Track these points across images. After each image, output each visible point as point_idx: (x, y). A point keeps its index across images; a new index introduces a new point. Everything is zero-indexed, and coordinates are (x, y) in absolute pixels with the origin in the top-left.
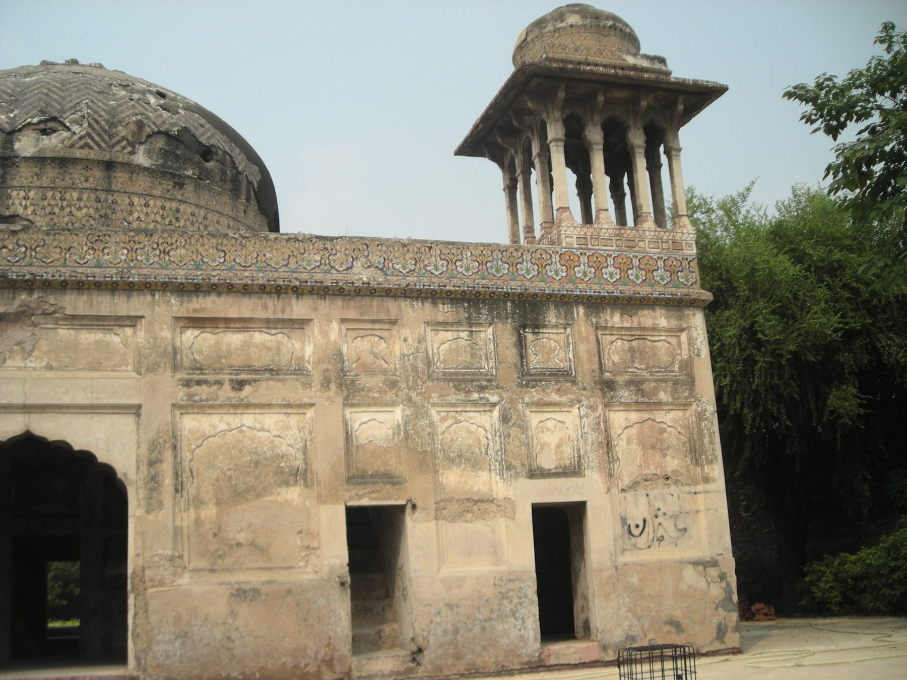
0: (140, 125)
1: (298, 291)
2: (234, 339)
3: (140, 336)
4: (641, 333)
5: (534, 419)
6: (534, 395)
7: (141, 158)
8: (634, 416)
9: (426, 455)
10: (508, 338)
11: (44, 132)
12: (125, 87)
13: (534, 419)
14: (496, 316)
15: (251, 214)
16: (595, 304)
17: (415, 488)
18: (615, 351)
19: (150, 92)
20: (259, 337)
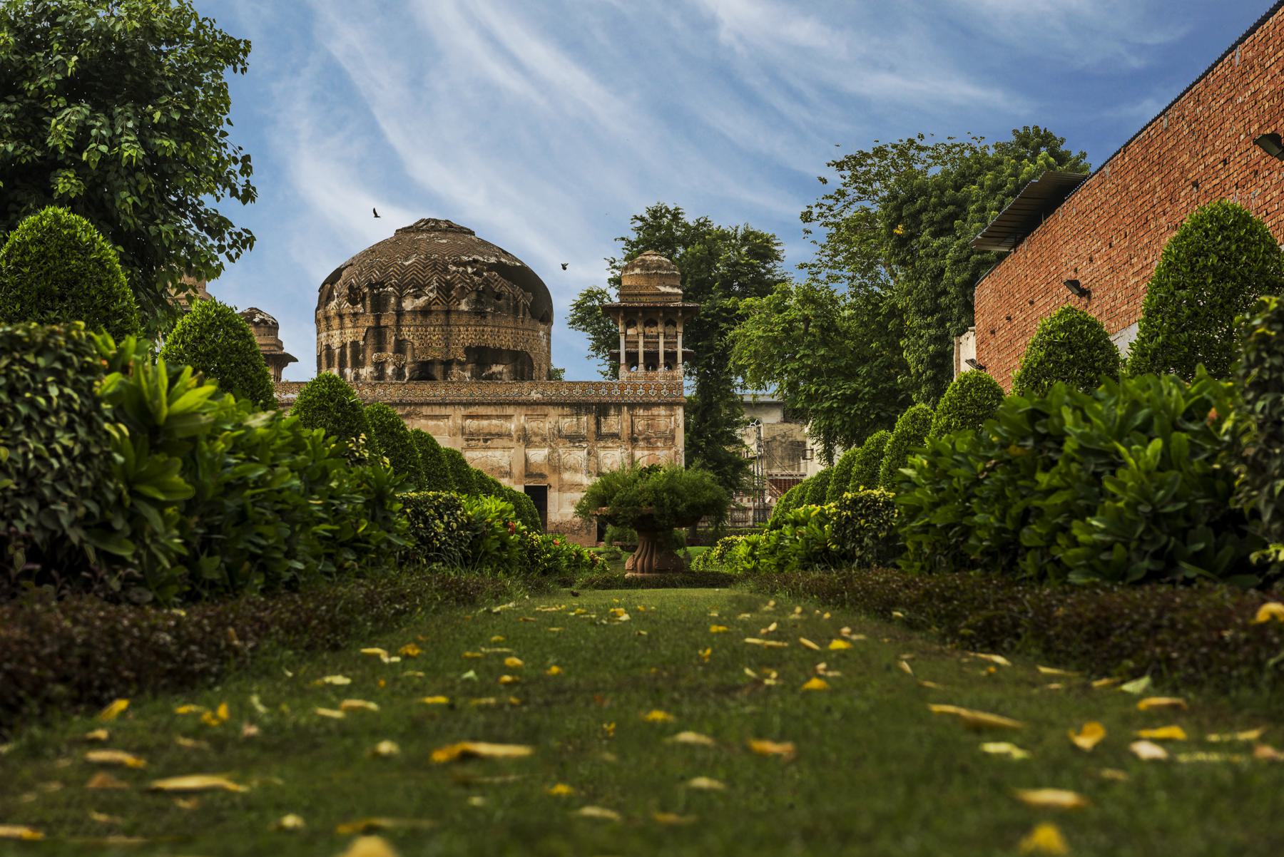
0: (462, 288)
1: (509, 404)
2: (485, 423)
3: (451, 422)
4: (653, 417)
5: (602, 453)
6: (602, 444)
7: (464, 307)
8: (646, 452)
9: (557, 467)
10: (592, 421)
11: (417, 297)
12: (455, 264)
13: (602, 453)
14: (588, 412)
15: (527, 321)
16: (632, 406)
17: (552, 480)
18: (640, 425)
19: (469, 263)
20: (494, 422)
